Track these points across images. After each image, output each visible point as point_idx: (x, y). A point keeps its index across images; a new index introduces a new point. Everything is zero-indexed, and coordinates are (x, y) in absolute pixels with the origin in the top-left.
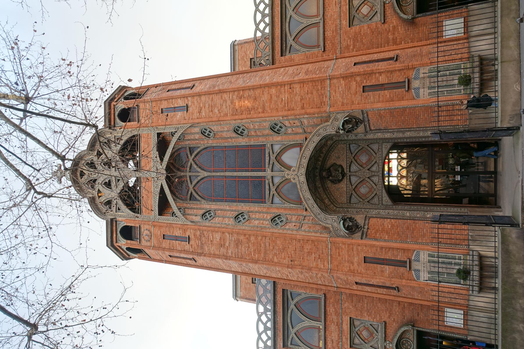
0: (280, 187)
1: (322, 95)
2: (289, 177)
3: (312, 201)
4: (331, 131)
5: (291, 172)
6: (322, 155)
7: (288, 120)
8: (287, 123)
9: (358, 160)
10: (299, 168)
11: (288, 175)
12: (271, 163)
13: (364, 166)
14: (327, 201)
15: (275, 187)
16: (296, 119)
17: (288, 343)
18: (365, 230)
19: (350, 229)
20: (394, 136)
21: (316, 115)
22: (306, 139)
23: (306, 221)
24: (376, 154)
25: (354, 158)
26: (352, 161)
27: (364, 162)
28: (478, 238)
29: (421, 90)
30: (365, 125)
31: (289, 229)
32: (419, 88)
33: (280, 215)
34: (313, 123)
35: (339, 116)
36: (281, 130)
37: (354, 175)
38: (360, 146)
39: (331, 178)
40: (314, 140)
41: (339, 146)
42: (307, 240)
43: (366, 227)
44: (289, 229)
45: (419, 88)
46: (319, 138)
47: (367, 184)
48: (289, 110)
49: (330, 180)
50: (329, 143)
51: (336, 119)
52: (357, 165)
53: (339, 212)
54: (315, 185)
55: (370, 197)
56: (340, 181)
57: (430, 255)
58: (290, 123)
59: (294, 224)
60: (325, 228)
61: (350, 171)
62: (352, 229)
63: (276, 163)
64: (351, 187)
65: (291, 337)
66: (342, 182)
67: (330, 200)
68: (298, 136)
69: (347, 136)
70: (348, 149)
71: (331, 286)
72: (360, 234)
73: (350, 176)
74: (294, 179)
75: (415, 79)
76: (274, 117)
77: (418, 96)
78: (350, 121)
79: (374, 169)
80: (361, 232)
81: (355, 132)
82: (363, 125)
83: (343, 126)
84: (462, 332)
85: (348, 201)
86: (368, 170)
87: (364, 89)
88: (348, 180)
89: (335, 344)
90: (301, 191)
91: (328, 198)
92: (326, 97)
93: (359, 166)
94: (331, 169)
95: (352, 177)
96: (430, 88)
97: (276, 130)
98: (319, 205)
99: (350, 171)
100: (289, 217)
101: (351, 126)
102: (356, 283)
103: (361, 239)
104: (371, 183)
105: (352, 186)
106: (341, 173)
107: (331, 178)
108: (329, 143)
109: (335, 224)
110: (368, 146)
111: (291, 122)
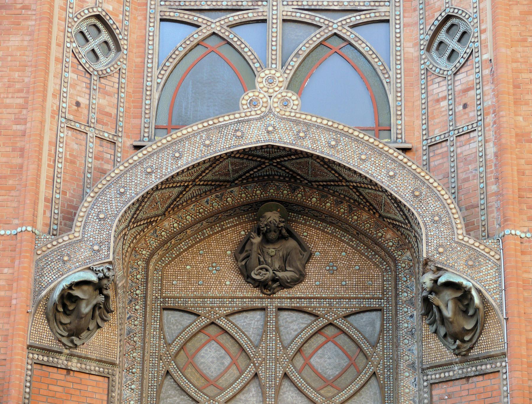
0: (226, 51)
2: (261, 81)
3: (169, 168)
4: (432, 242)
5: (279, 90)
6: (343, 209)
7: (480, 82)
8: (464, 78)
9: (320, 339)
10: (297, 122)
11: (271, 81)
12: (318, 18)
13: (299, 361)
14: (170, 224)
15: (226, 34)
16: (483, 113)
18: (62, 361)
19: (64, 306)
21: (493, 188)
22: (405, 150)
26: (317, 316)
27: (314, 361)
30: (450, 364)
31: (63, 81)
33: (118, 48)
34: (462, 176)
36: (441, 55)
37: (266, 322)
38: (374, 346)
39: (257, 240)
40: (398, 181)
41: (376, 272)
42: (22, 150)
43: (74, 364)
44: (63, 81)
46: (404, 196)
47: (234, 371)
48: (516, 86)
49: (248, 239)
50: (389, 237)
51: (474, 260)
52: (305, 335)
53: (129, 269)
54: (232, 183)
55: (184, 382)
56: (245, 273)
58: (466, 91)
59: (84, 101)
60: (68, 218)
61: (280, 309)
62: (66, 312)
63: (317, 36)
64: (223, 312)
66: (240, 280)
67: (173, 236)
68: (418, 122)
69: (411, 302)
70: (365, 304)
72: (47, 339)
73: (263, 309)
74: (253, 103)
76: (494, 28)
78: (465, 312)
80: (56, 346)
81: (427, 330)
82: (449, 356)
83: (449, 285)
85: (170, 304)
86: (286, 375)
88: (248, 303)
90: (207, 130)
91: (182, 230)
93: (299, 341)
94: (291, 243)
95: (258, 315)
97: (442, 36)
98: (157, 194)
99: (280, 309)
100: (111, 84)
101: (448, 313)
103: (30, 347)
104: (237, 386)
105: (227, 316)
106: (274, 280)
107: (257, 240)
108: (389, 237)
109: (84, 253)
110: (374, 374)
111: (472, 93)
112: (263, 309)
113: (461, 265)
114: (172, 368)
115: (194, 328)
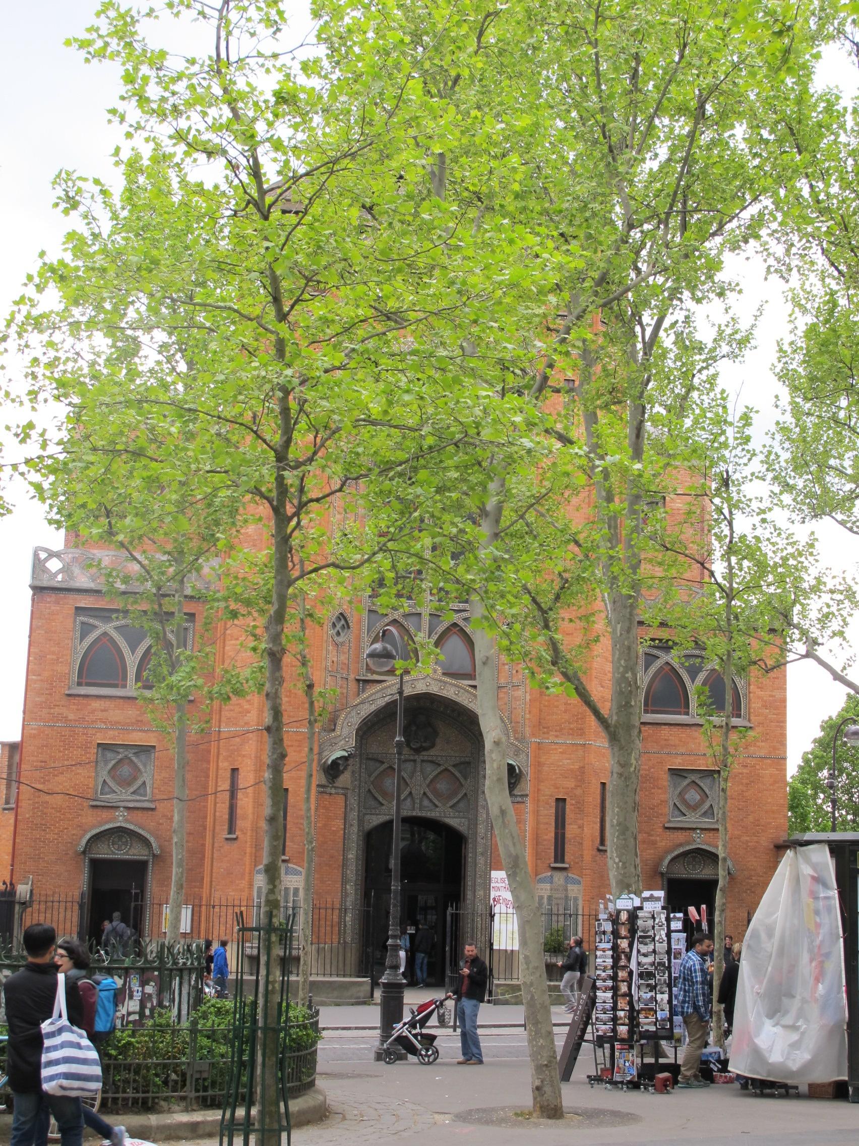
1: (561, 730)
10: (440, 681)
17: (85, 616)
20: (479, 839)
23: (340, 682)
24: (451, 807)
25: (446, 770)
28: (322, 956)
29: (548, 886)
31: (327, 651)
32: (551, 883)
33: (349, 627)
35: (522, 757)
43: (333, 791)
44: (327, 651)
45: (551, 883)
57: (296, 890)
61: (423, 761)
65: (96, 623)
71: (220, 721)
72: (324, 781)
73: (415, 761)
75: (567, 878)
77: (541, 881)
79: (426, 802)
84: (155, 929)
86: (425, 794)
87: (561, 802)
89: (100, 715)
92: (556, 736)
96: (550, 898)
102: (234, 771)
106: (421, 747)
107: (414, 728)
112: (415, 761)
113: (511, 754)
114: (371, 787)
115: (381, 769)
